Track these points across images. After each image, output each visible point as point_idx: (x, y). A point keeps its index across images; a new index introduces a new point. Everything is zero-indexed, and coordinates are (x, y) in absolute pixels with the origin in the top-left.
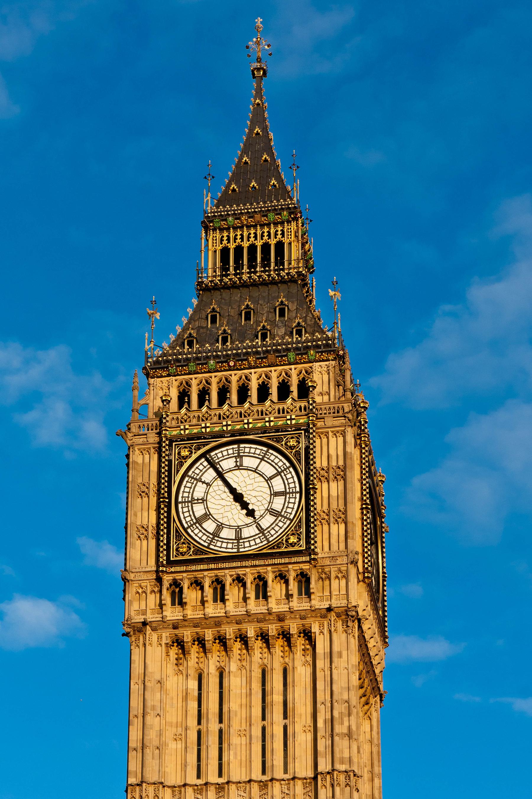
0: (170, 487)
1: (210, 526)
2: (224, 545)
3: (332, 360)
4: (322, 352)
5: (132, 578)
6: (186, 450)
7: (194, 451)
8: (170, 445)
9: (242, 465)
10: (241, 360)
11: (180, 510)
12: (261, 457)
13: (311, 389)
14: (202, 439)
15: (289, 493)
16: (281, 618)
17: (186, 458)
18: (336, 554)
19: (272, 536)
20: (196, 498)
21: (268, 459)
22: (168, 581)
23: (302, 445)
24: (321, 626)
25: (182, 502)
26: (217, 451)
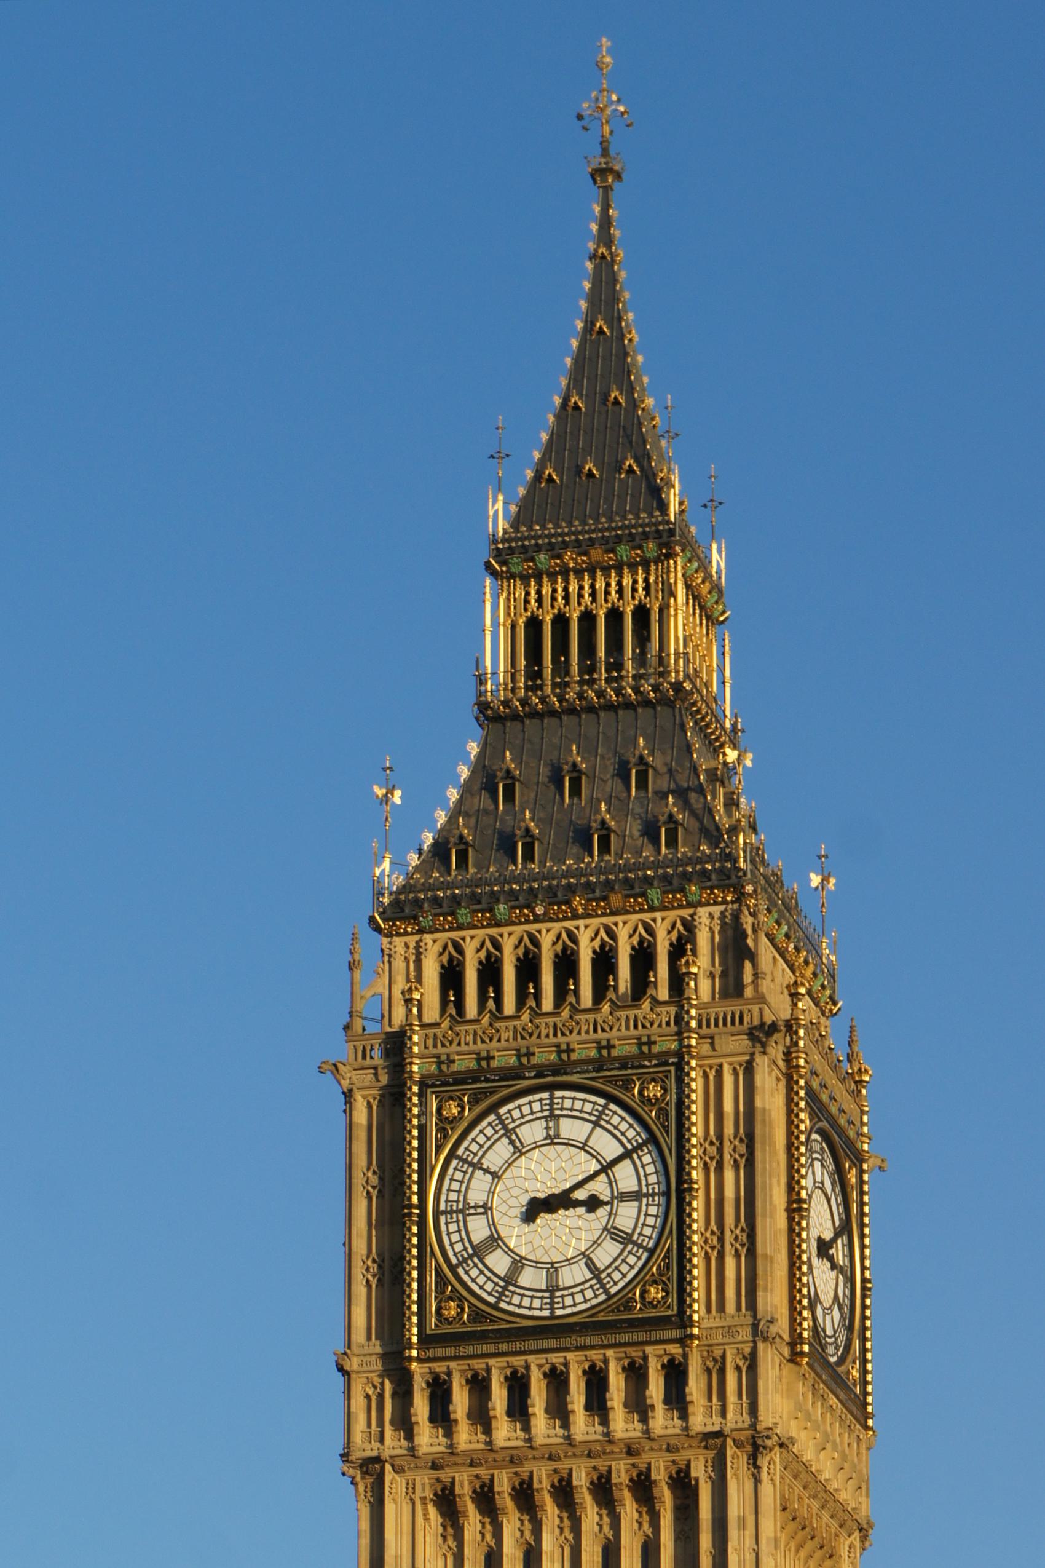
1: (499, 1262)
2: (526, 1302)
5: (355, 1367)
8: (421, 1095)
9: (557, 1136)
10: (559, 898)
11: (443, 1228)
12: (593, 1118)
13: (687, 980)
14: (482, 1082)
15: (647, 1195)
19: (615, 1284)
20: (472, 1204)
21: (608, 1122)
25: (445, 1212)
26: (511, 1106)
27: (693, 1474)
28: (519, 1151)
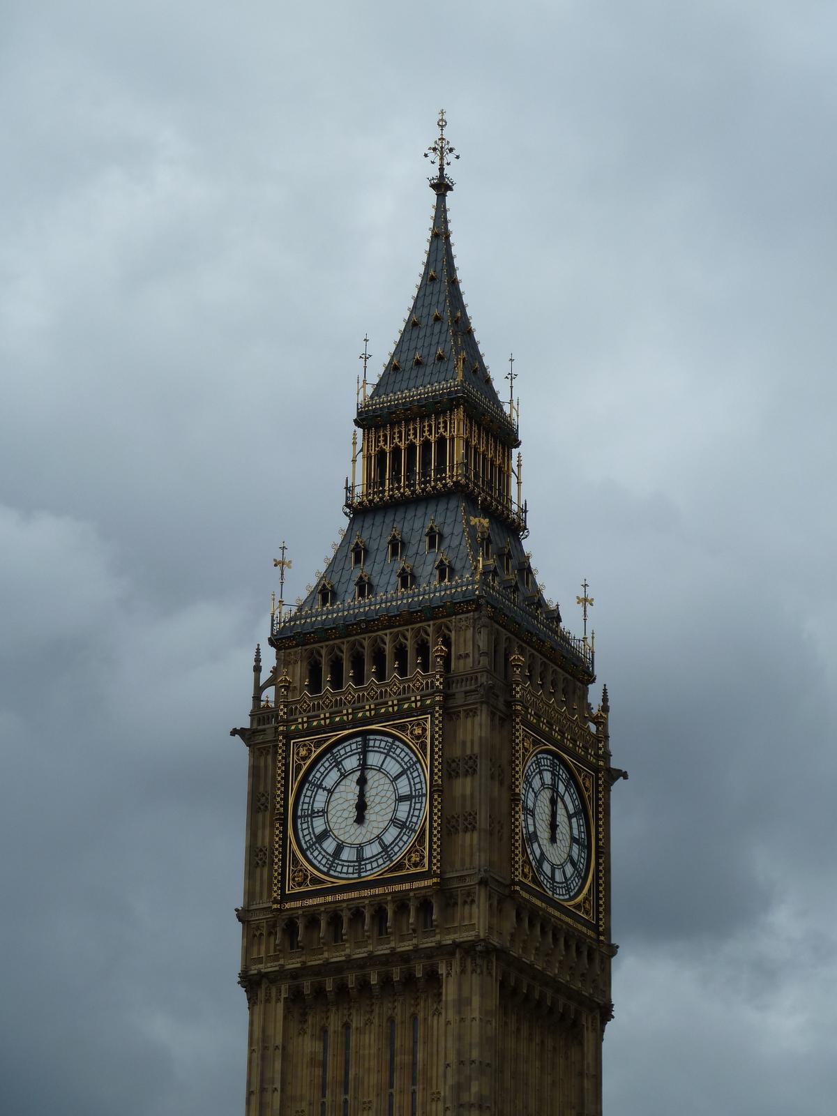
0: (286, 799)
1: (329, 845)
2: (345, 870)
3: (474, 611)
4: (460, 603)
6: (305, 748)
7: (313, 749)
12: (386, 751)
16: (405, 958)
17: (304, 758)
18: (465, 873)
20: (316, 810)
22: (283, 920)
23: (428, 733)
24: (449, 965)
25: (301, 817)
27: (440, 973)
28: (344, 776)
